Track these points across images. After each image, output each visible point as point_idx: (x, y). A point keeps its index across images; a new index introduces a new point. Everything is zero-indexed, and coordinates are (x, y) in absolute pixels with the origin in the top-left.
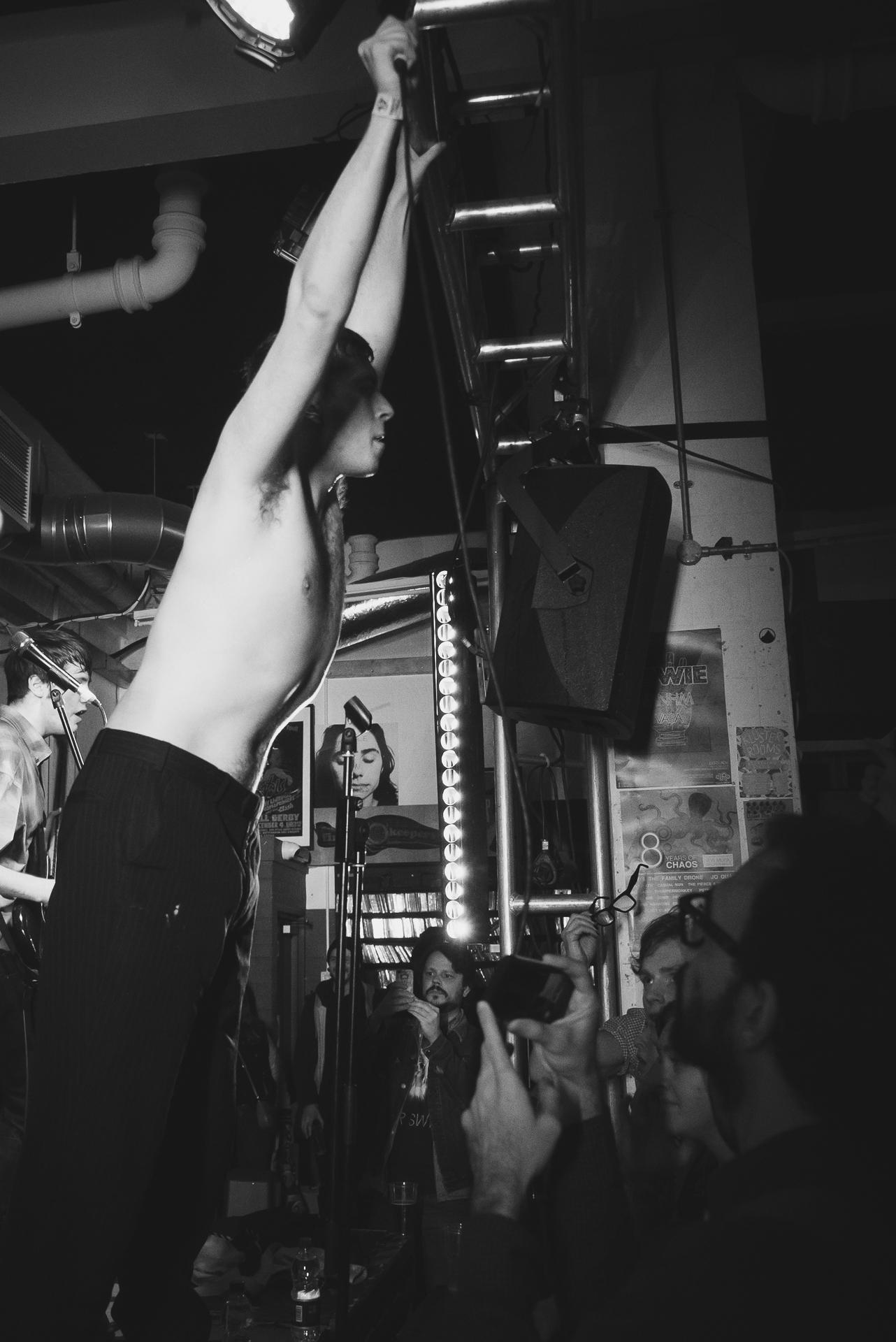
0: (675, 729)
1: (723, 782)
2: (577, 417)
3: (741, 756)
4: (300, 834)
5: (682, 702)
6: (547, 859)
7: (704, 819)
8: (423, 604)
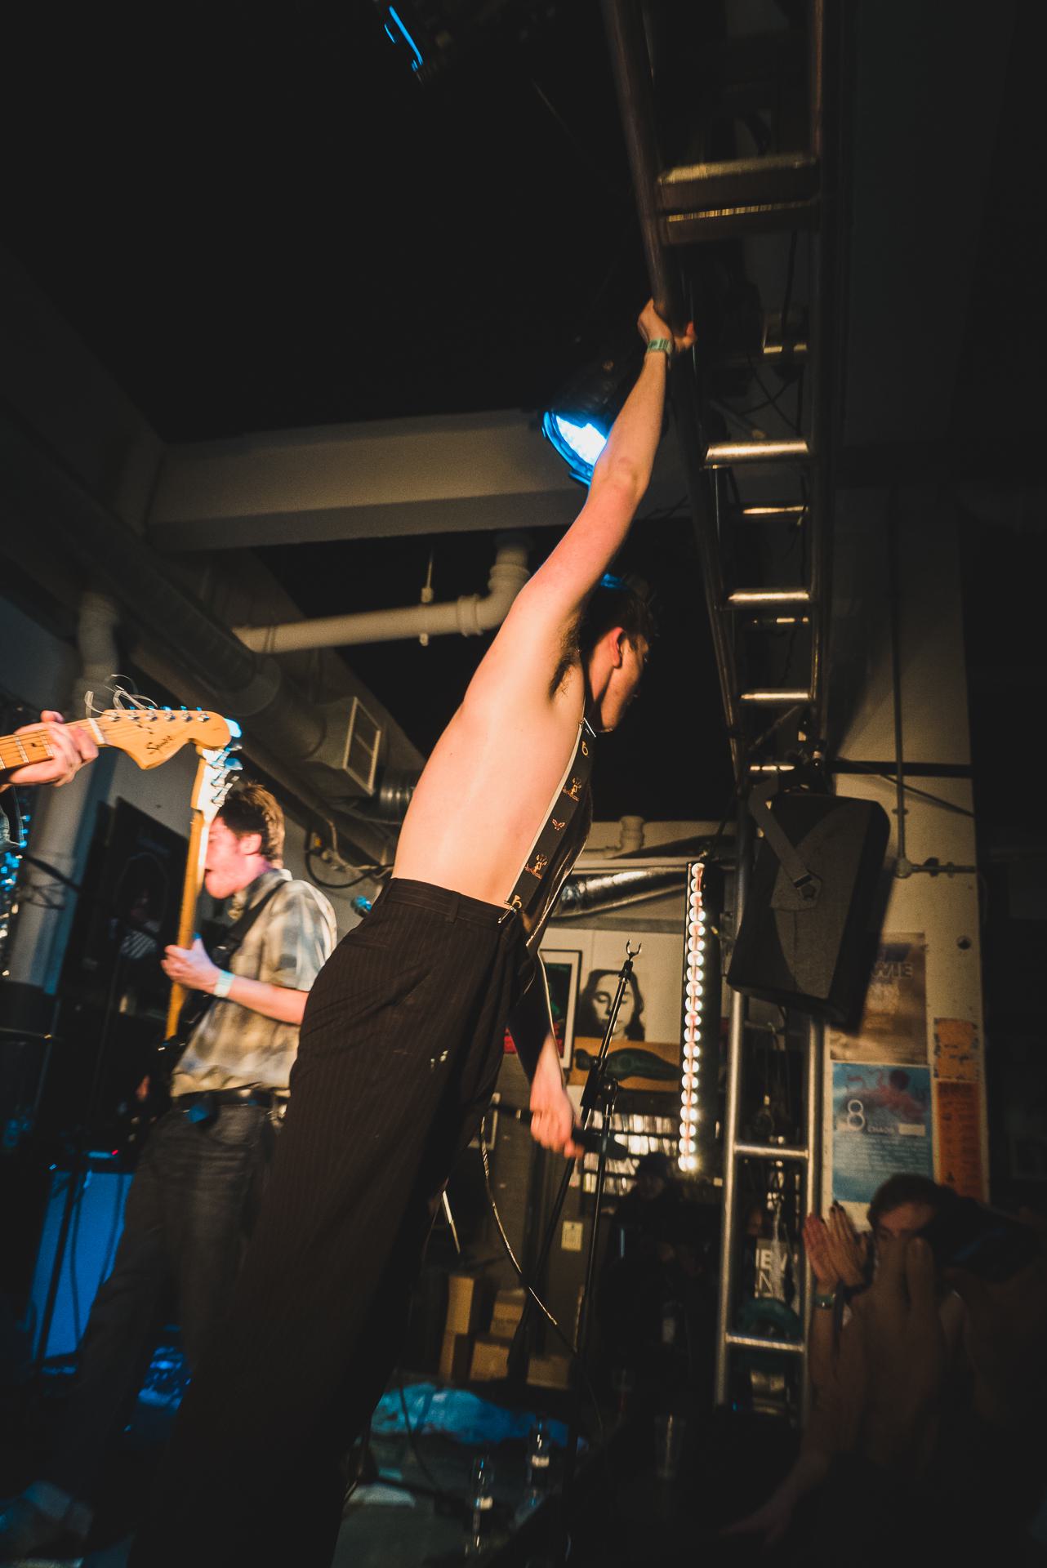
0: (883, 1014)
2: (816, 754)
6: (767, 1112)
8: (680, 879)
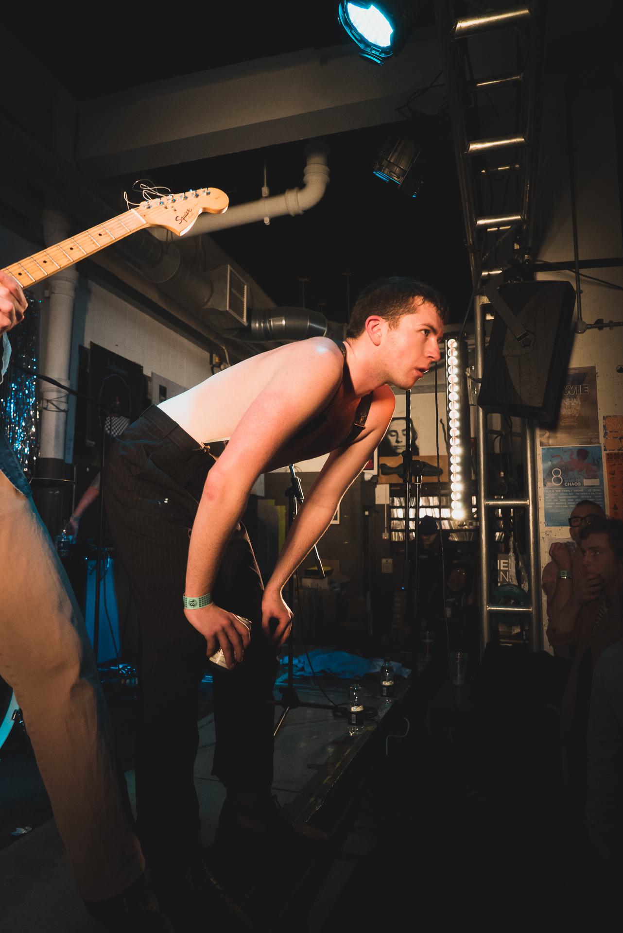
0: (571, 417)
1: (595, 443)
3: (605, 430)
4: (373, 469)
5: (575, 403)
7: (585, 462)
